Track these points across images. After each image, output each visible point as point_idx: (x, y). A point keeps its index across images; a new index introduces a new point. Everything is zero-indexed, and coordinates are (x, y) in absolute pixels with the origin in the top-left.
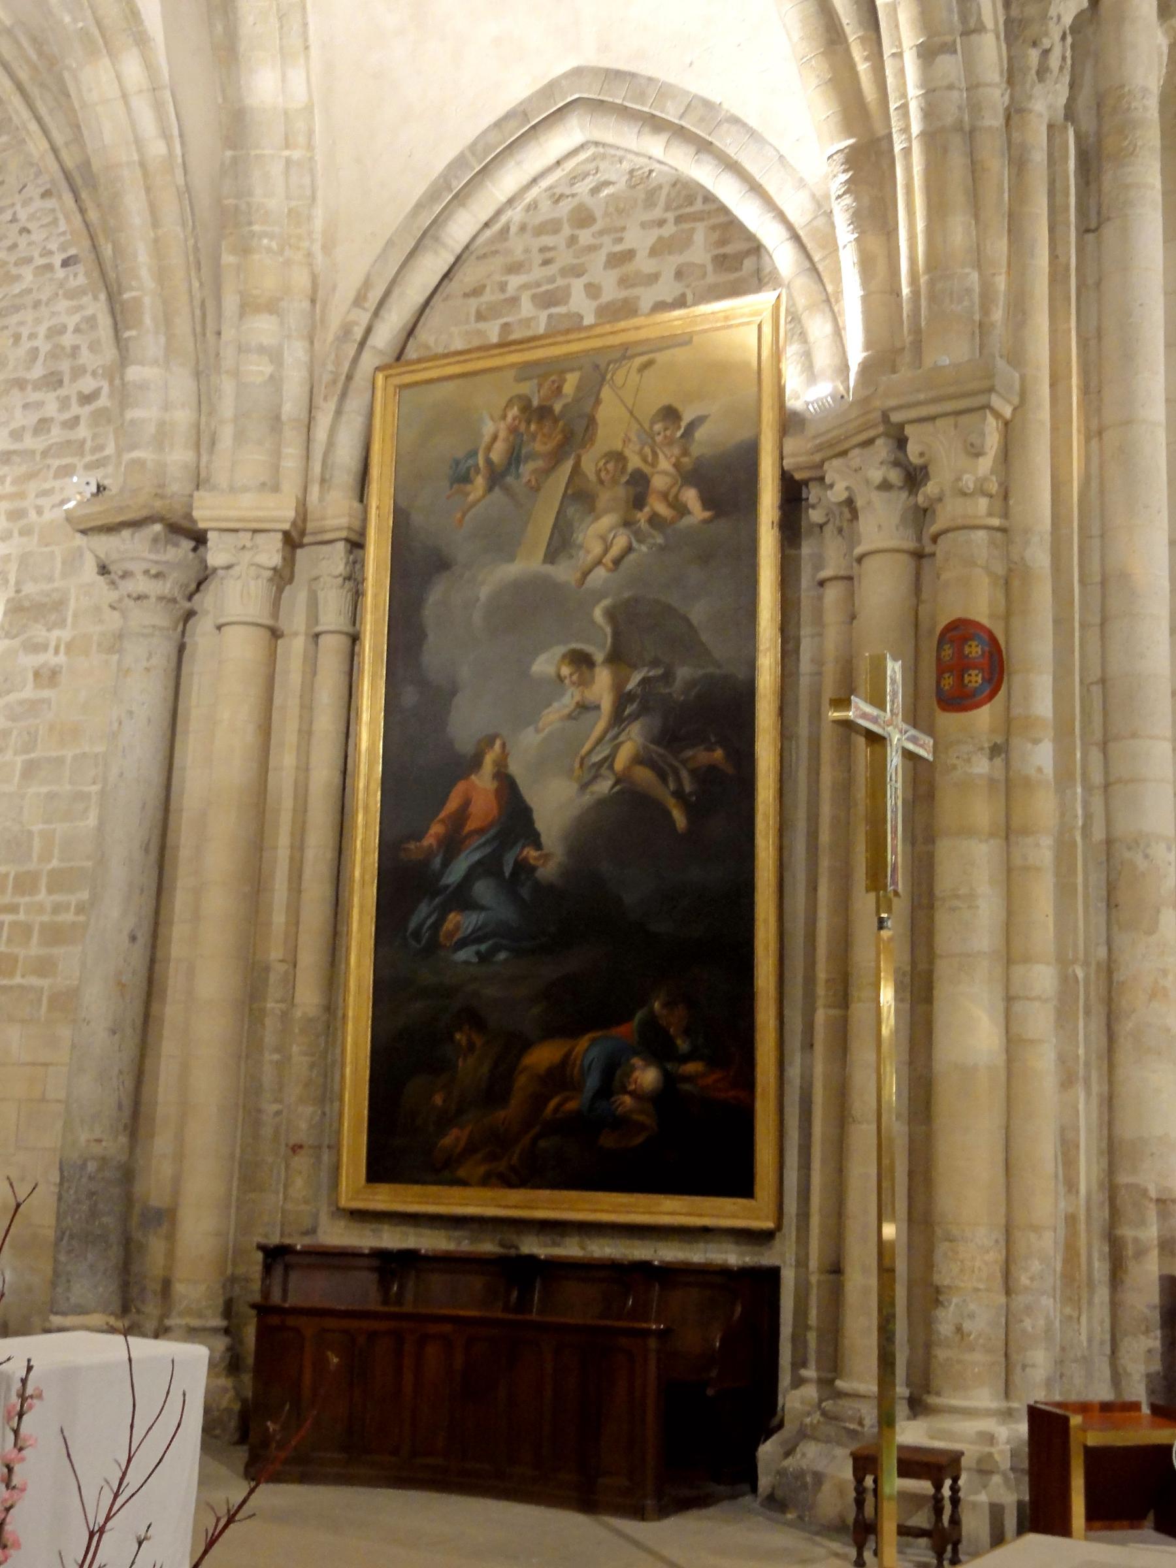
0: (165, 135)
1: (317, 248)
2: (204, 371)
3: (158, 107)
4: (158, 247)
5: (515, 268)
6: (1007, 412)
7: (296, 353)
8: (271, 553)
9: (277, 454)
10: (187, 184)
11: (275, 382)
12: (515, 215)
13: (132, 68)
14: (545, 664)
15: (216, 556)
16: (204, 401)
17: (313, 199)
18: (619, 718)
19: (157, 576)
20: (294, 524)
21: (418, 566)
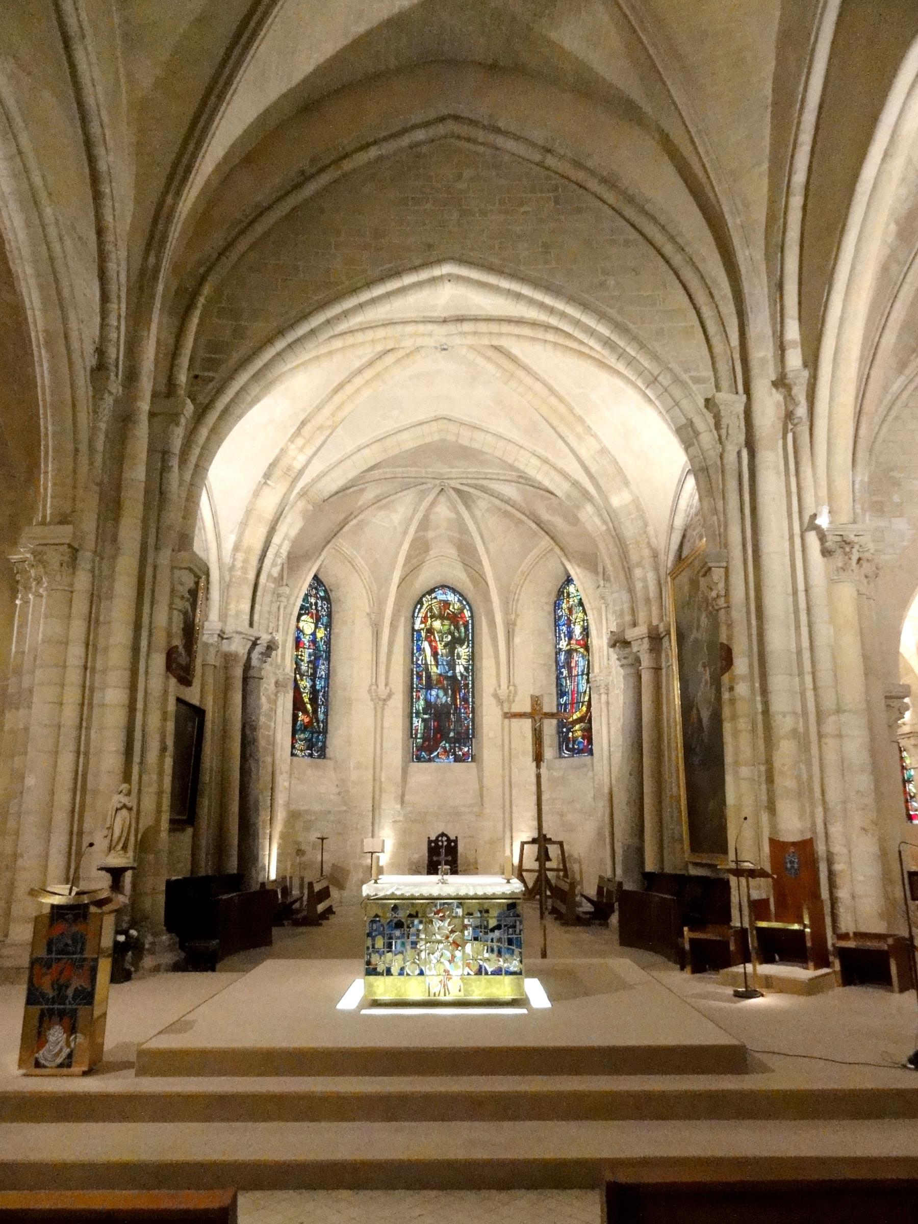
0: (605, 522)
1: (653, 541)
2: (631, 591)
3: (600, 516)
4: (611, 558)
5: (694, 530)
6: (725, 564)
7: (651, 576)
8: (646, 644)
9: (650, 610)
10: (617, 535)
11: (646, 588)
12: (693, 511)
13: (589, 508)
14: (700, 669)
15: (635, 649)
16: (633, 600)
17: (646, 525)
18: (711, 685)
19: (625, 658)
20: (649, 632)
21: (681, 638)
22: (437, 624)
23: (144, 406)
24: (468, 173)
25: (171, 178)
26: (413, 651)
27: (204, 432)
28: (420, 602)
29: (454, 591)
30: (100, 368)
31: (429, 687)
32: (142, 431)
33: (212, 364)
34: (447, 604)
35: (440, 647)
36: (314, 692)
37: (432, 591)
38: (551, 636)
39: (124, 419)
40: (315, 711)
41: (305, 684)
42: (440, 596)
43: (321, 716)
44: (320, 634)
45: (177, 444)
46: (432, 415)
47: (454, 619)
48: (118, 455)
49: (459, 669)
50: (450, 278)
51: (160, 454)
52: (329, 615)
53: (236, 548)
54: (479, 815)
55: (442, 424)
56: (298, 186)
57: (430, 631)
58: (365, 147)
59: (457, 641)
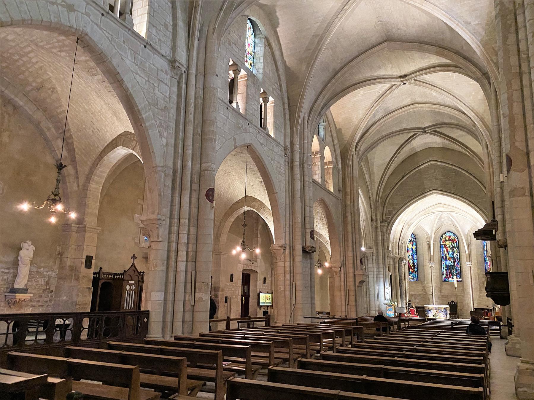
22: (447, 243)
23: (379, 225)
24: (436, 171)
25: (380, 183)
26: (441, 250)
27: (389, 227)
28: (442, 236)
29: (452, 233)
30: (372, 220)
31: (446, 260)
32: (379, 230)
33: (390, 214)
34: (450, 237)
35: (449, 249)
36: (413, 263)
37: (445, 233)
38: (482, 246)
39: (376, 228)
40: (414, 269)
41: (411, 261)
42: (448, 234)
43: (416, 270)
44: (414, 248)
45: (385, 230)
46: (436, 203)
47: (452, 241)
48: (376, 236)
49: (455, 255)
50: (434, 193)
51: (382, 232)
52: (416, 243)
53: (394, 238)
54: (463, 296)
55: (439, 205)
56: (402, 178)
57: (445, 245)
58: (415, 169)
59: (453, 247)
